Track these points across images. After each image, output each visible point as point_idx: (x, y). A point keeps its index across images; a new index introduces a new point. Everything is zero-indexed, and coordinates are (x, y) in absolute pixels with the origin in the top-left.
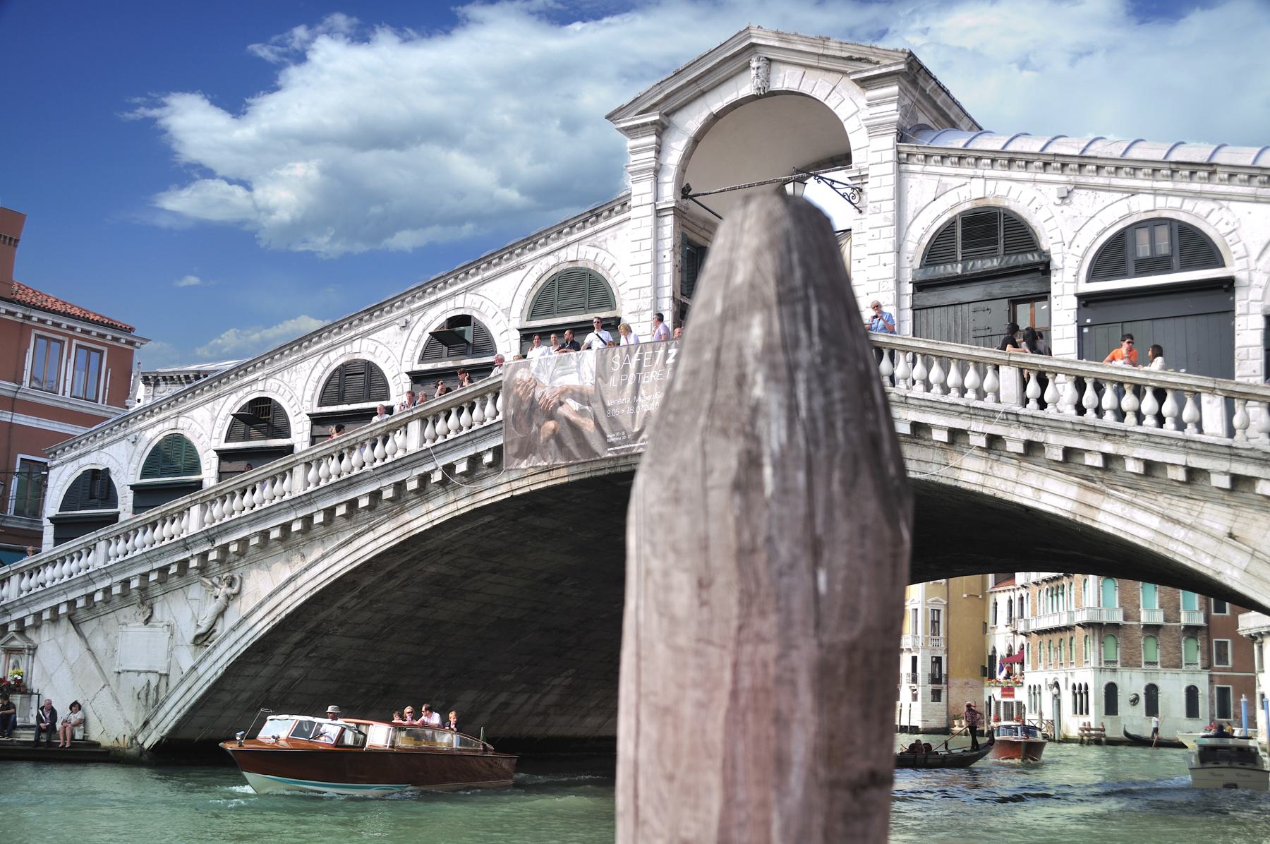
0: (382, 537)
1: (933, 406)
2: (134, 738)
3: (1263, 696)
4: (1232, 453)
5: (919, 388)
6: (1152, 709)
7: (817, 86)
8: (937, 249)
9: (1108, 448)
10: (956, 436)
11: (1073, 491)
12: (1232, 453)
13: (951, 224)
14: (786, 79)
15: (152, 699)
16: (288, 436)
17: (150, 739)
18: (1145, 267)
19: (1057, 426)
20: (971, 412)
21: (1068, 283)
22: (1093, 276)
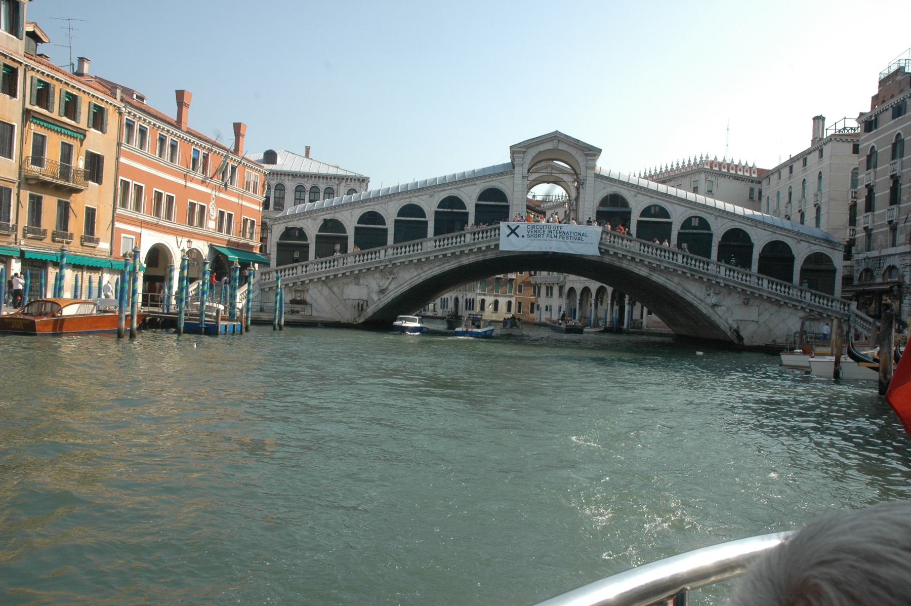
0: (452, 265)
3: (538, 306)
4: (684, 267)
8: (604, 202)
11: (647, 271)
13: (607, 197)
14: (562, 147)
15: (361, 307)
17: (361, 320)
19: (648, 257)
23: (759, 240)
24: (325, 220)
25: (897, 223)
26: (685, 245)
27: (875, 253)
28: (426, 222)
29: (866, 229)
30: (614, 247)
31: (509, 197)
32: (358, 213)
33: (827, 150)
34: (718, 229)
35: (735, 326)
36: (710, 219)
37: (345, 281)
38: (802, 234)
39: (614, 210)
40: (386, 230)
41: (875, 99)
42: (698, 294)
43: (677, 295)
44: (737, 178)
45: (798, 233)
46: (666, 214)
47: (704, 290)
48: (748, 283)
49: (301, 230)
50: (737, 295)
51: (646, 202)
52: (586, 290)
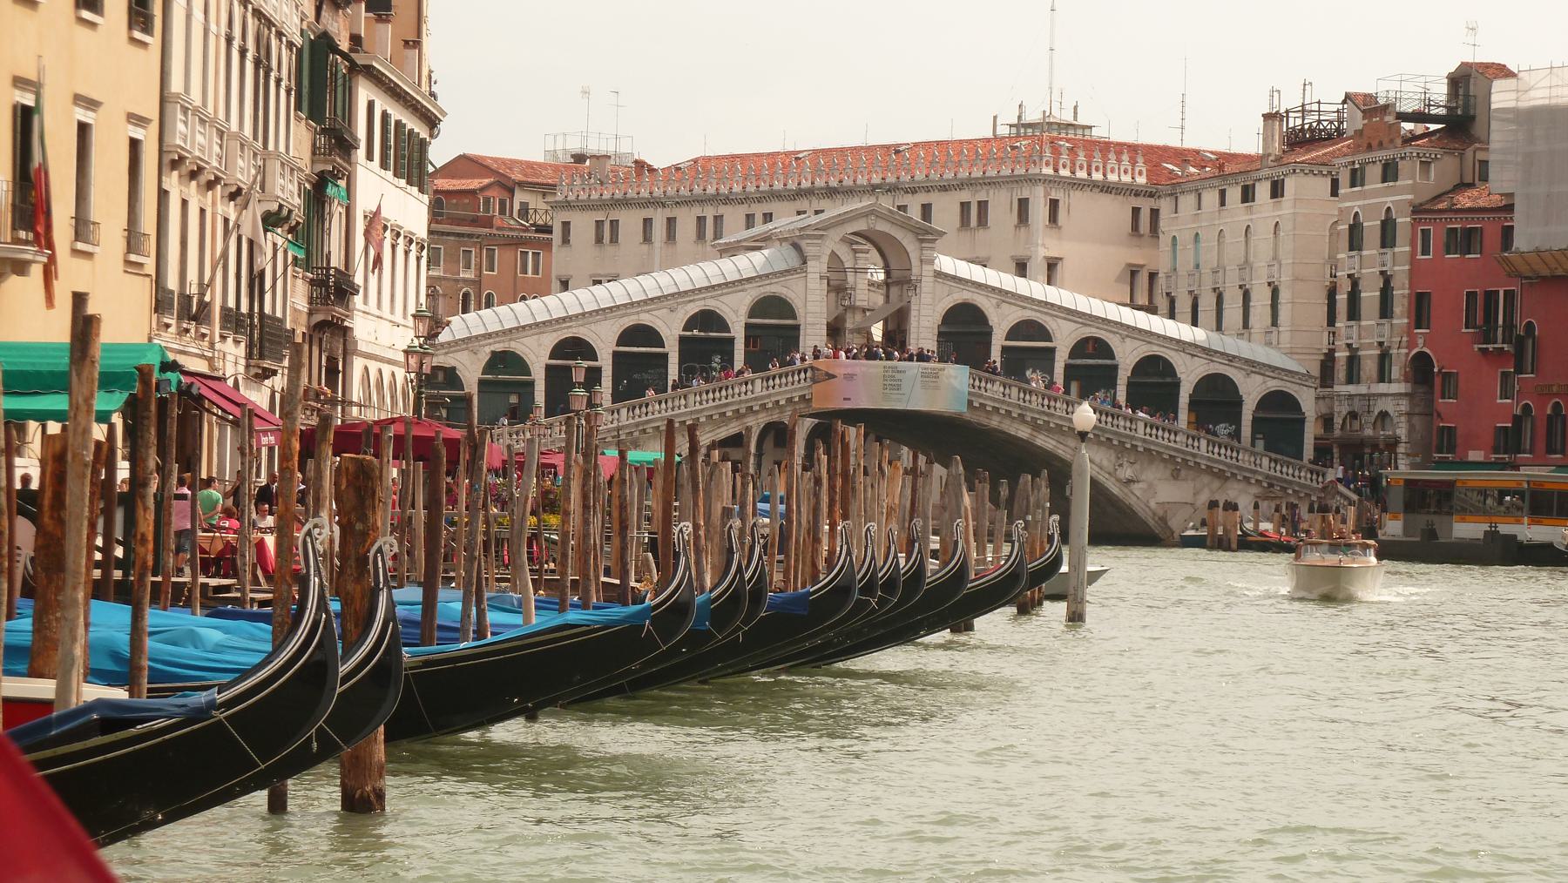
7: (898, 234)
10: (996, 410)
14: (882, 227)
23: (1189, 373)
26: (1074, 387)
27: (1362, 389)
28: (665, 356)
30: (981, 396)
31: (800, 312)
32: (550, 340)
33: (1290, 184)
35: (1161, 513)
36: (1113, 341)
39: (964, 332)
42: (1105, 463)
44: (1106, 188)
45: (1247, 361)
46: (1047, 336)
47: (1113, 458)
50: (1162, 466)
51: (1014, 315)
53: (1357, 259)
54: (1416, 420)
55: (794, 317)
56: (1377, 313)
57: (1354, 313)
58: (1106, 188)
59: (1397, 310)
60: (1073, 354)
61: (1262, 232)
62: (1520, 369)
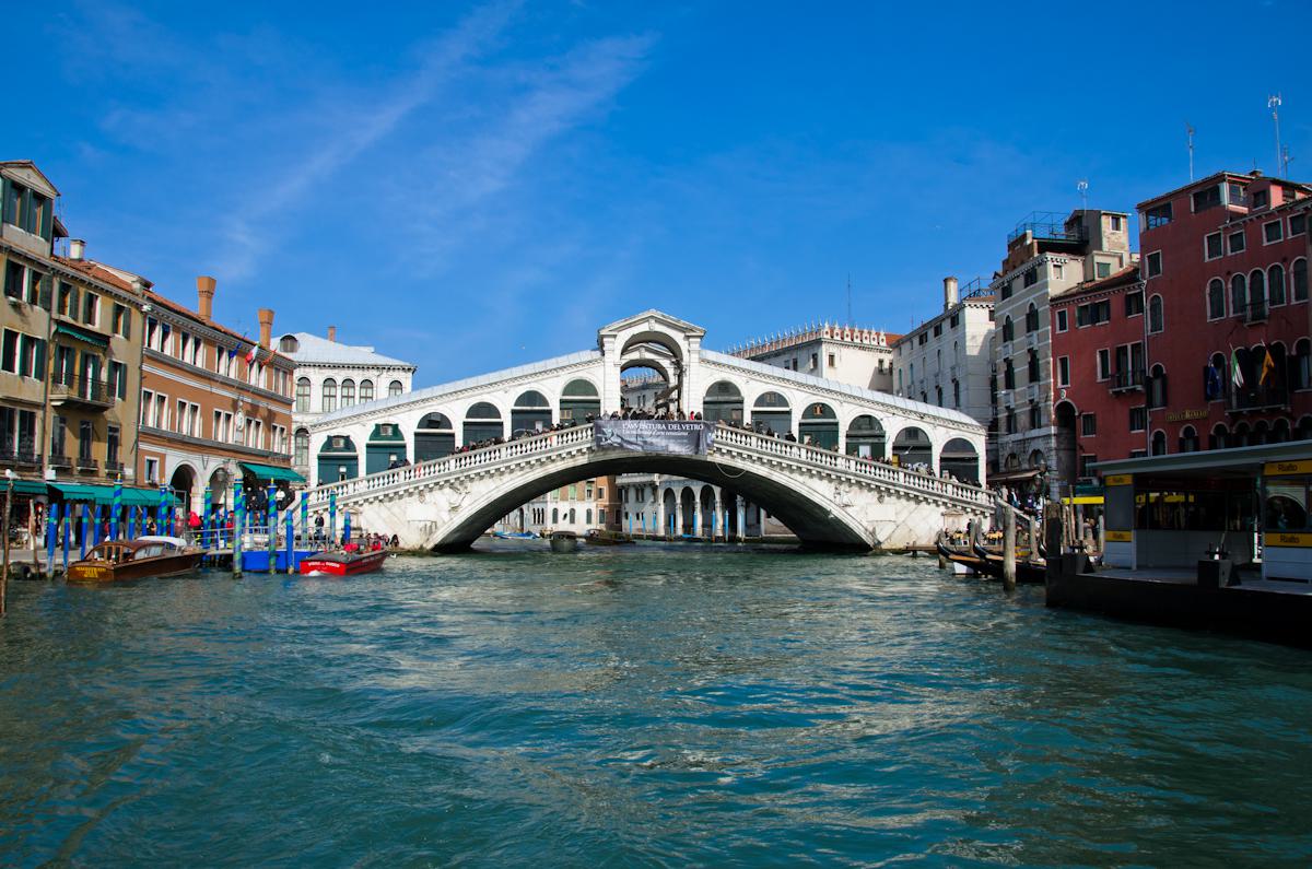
0: (539, 473)
1: (734, 446)
2: (421, 547)
3: (627, 514)
4: (808, 464)
5: (729, 440)
6: (572, 521)
8: (710, 392)
9: (779, 460)
12: (808, 464)
15: (430, 529)
16: (451, 428)
17: (429, 546)
18: (768, 405)
20: (745, 449)
21: (749, 407)
22: (756, 405)
23: (892, 427)
24: (377, 425)
25: (1038, 403)
27: (1018, 436)
28: (501, 424)
29: (1008, 408)
32: (418, 414)
34: (845, 416)
36: (834, 405)
37: (406, 499)
38: (939, 418)
40: (453, 435)
41: (1005, 263)
43: (803, 496)
45: (934, 417)
48: (882, 478)
49: (347, 439)
52: (688, 495)
53: (1010, 346)
54: (1061, 454)
55: (596, 394)
56: (1027, 380)
57: (1010, 384)
58: (862, 348)
59: (1042, 374)
60: (804, 416)
61: (948, 348)
62: (1150, 404)
